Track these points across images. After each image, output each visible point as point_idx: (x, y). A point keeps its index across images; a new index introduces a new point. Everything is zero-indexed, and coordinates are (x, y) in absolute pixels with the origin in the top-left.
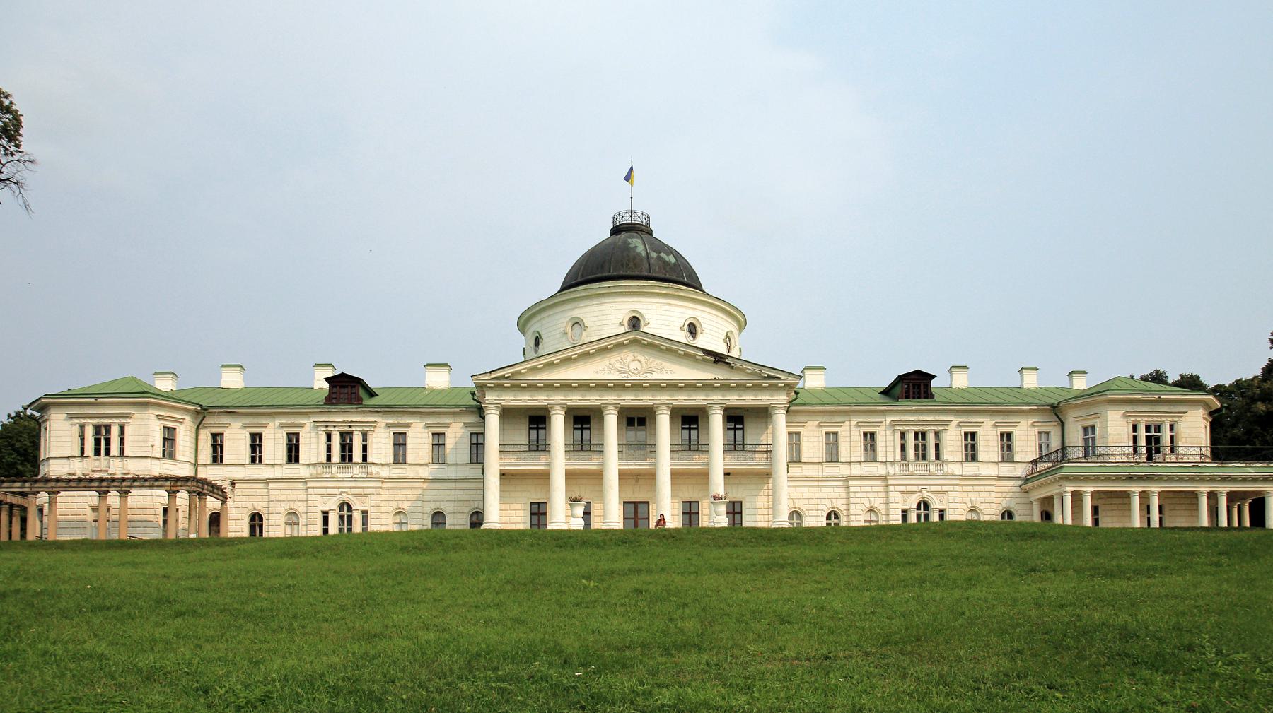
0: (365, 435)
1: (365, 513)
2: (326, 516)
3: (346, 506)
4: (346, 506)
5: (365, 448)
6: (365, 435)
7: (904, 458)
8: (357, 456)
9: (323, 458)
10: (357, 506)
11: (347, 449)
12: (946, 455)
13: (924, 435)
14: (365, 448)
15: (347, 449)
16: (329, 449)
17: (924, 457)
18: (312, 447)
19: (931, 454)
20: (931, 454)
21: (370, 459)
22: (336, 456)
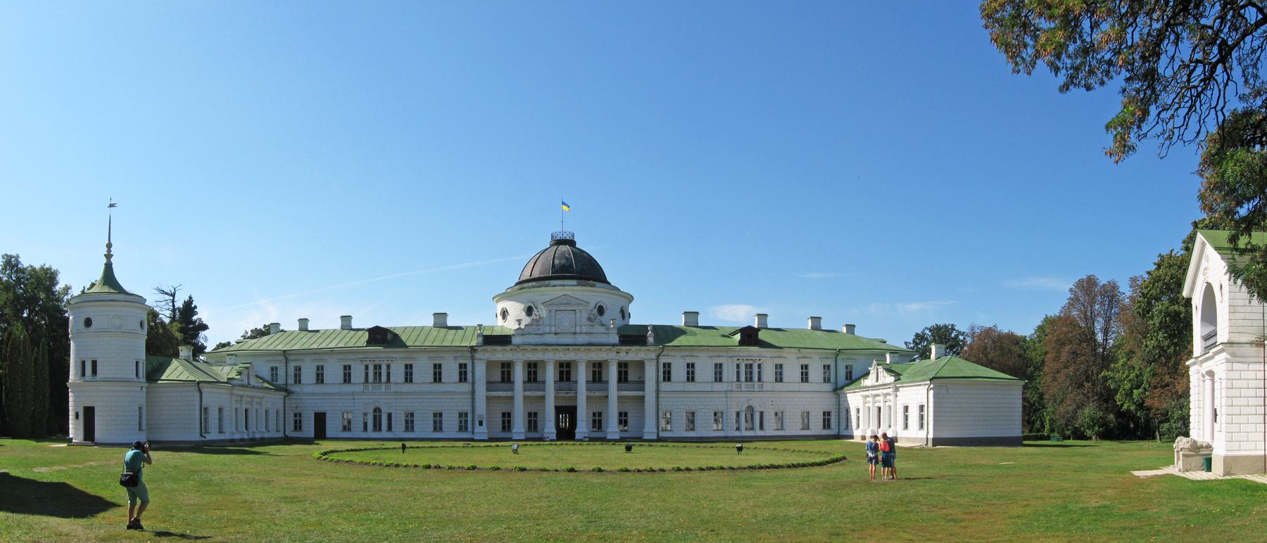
0: (388, 366)
1: (390, 416)
2: (365, 414)
3: (377, 410)
4: (377, 410)
5: (388, 374)
6: (388, 366)
7: (738, 380)
8: (384, 378)
9: (363, 380)
10: (385, 411)
11: (378, 375)
12: (764, 378)
13: (751, 366)
14: (388, 374)
15: (378, 375)
16: (367, 375)
17: (751, 380)
18: (358, 374)
19: (756, 377)
20: (756, 377)
21: (392, 379)
22: (371, 379)
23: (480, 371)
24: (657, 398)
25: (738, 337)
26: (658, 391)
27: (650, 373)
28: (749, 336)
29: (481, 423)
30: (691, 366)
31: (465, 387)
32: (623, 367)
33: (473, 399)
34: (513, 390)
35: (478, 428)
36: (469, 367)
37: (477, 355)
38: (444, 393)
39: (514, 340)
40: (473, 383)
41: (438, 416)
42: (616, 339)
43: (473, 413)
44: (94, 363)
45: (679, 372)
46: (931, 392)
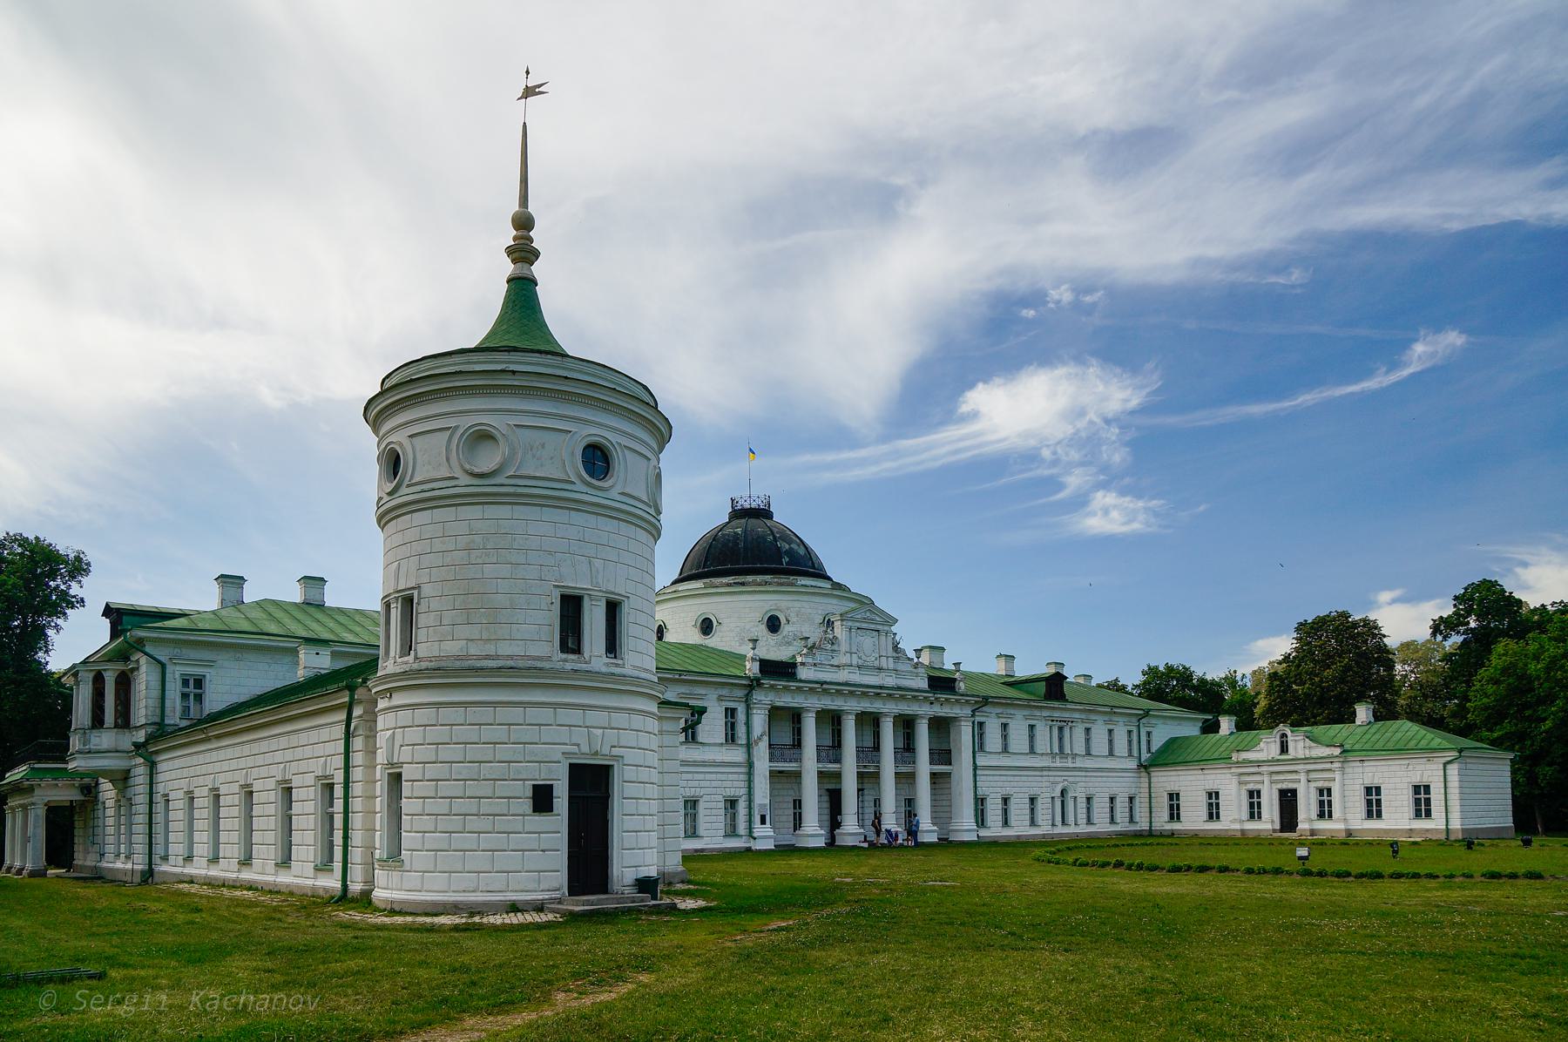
23: (759, 721)
24: (975, 775)
25: (1042, 687)
26: (975, 768)
27: (965, 733)
28: (1055, 686)
29: (763, 821)
30: (1005, 726)
31: (738, 755)
32: (941, 726)
33: (750, 774)
34: (799, 760)
35: (759, 830)
36: (741, 716)
37: (758, 696)
38: (704, 764)
39: (803, 673)
40: (749, 746)
41: (692, 804)
42: (924, 684)
43: (750, 801)
44: (613, 608)
45: (993, 739)
46: (1453, 770)
